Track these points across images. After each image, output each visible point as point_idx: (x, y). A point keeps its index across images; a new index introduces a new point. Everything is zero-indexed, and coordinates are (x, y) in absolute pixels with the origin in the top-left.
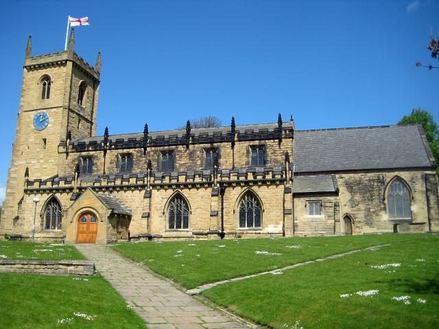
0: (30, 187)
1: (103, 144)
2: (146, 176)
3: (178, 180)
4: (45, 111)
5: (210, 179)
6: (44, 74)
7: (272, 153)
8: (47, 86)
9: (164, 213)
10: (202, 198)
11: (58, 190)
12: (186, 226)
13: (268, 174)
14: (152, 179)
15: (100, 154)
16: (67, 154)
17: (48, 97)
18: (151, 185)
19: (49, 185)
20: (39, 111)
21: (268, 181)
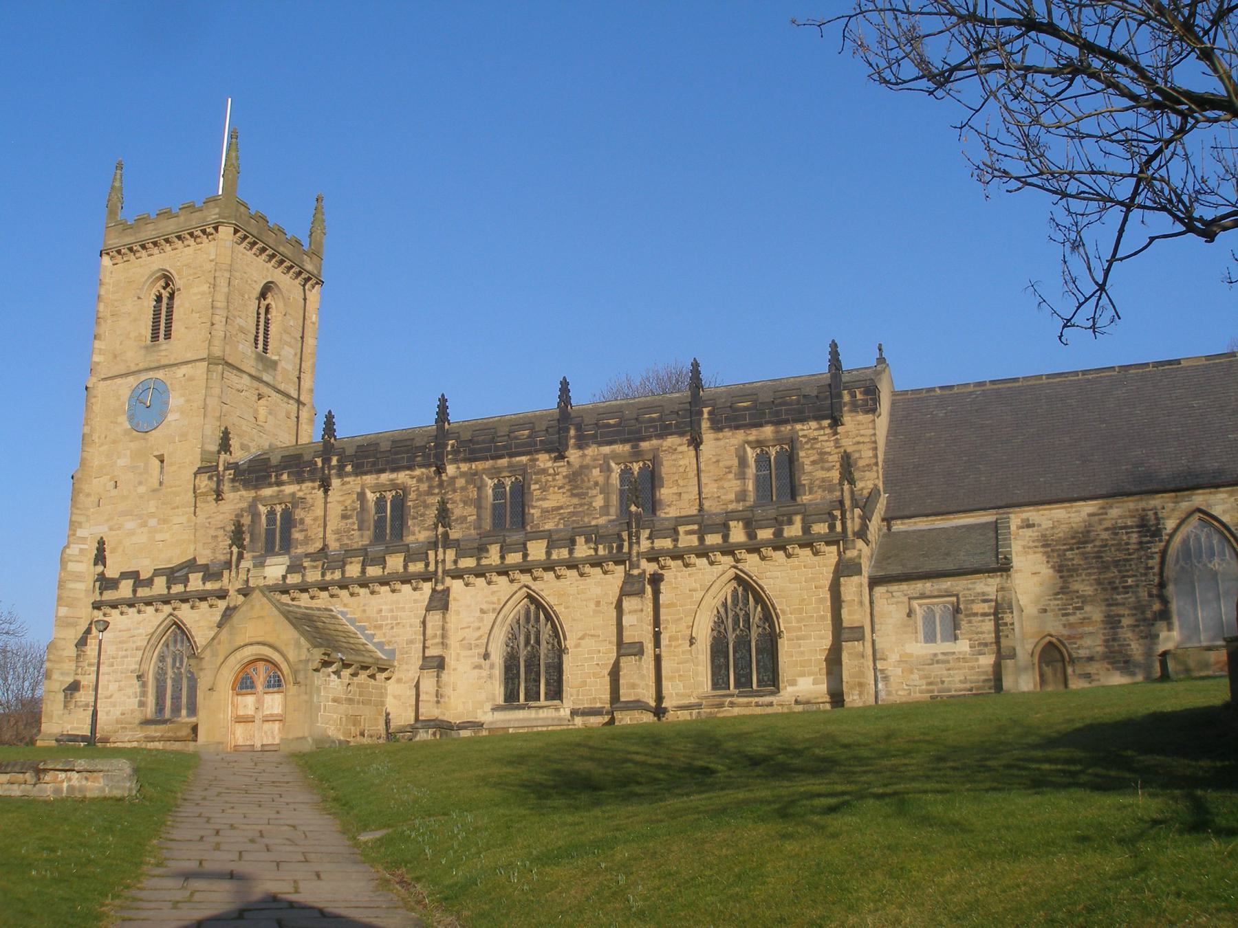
0: (109, 595)
2: (434, 545)
3: (525, 556)
4: (160, 374)
5: (620, 547)
6: (155, 267)
7: (814, 463)
8: (165, 301)
9: (486, 656)
10: (598, 603)
12: (556, 693)
13: (790, 522)
14: (451, 554)
15: (308, 490)
17: (168, 336)
18: (446, 573)
19: (160, 586)
20: (143, 377)
21: (791, 541)
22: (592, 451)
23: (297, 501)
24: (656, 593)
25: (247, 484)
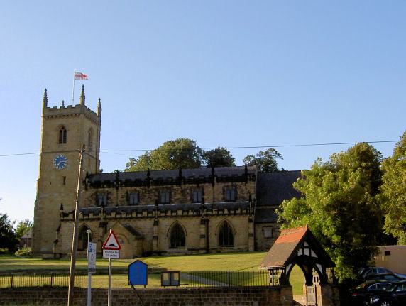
1: (115, 183)
2: (155, 210)
11: (88, 220)
12: (183, 244)
14: (159, 212)
15: (113, 190)
16: (86, 189)
17: (65, 143)
22: (187, 185)
23: (109, 193)
24: (208, 224)
25: (94, 187)
